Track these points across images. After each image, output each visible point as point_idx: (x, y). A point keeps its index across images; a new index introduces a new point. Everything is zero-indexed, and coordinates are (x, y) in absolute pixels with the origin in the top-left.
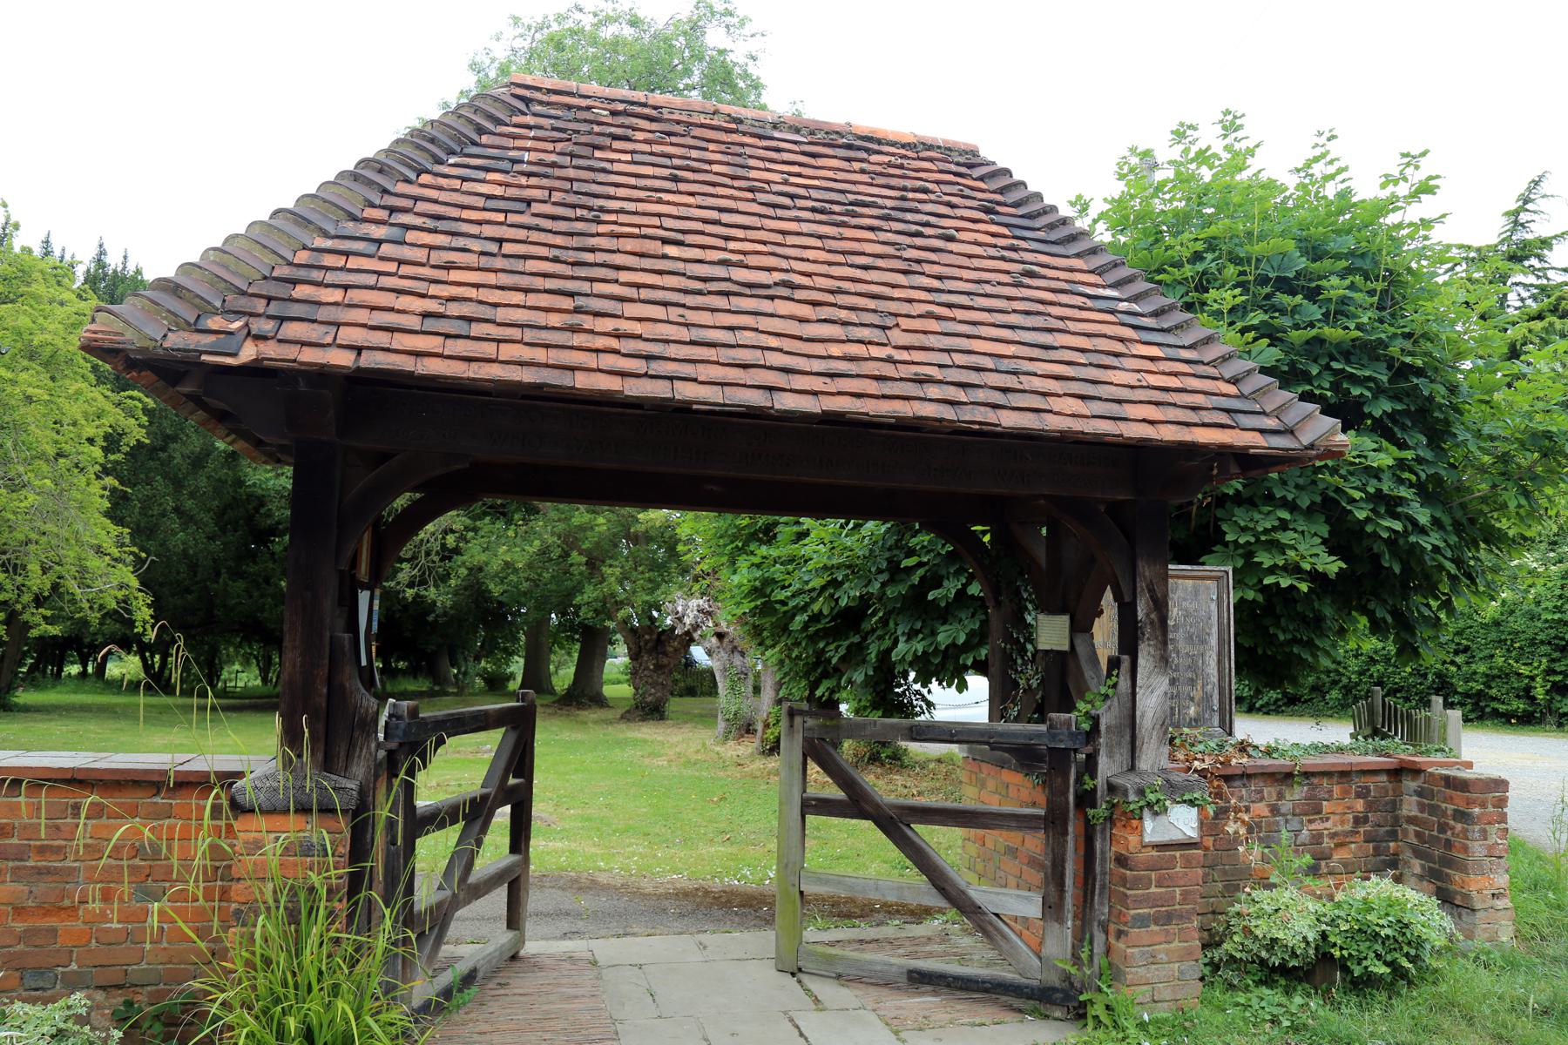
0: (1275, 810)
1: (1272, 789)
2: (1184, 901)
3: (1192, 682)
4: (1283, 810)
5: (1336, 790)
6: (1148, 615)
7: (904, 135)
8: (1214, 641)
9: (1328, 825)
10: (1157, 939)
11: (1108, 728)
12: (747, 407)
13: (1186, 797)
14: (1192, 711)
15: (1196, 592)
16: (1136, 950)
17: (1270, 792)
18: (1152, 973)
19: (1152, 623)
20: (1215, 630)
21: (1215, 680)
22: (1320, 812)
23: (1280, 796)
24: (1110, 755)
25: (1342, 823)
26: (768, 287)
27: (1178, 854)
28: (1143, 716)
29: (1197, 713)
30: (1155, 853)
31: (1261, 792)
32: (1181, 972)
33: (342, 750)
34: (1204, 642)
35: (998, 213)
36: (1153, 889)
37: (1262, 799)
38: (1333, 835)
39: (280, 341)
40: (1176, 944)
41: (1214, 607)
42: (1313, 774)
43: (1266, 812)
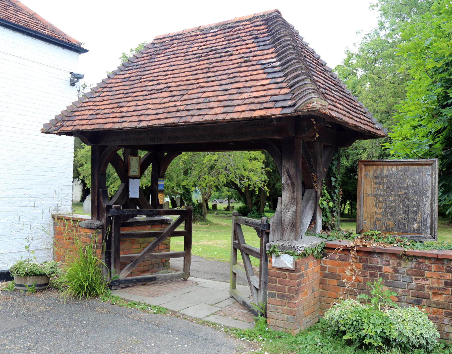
0: (396, 271)
1: (395, 261)
2: (289, 292)
3: (416, 213)
4: (400, 271)
5: (433, 267)
6: (286, 182)
7: (244, 17)
8: (429, 194)
9: (427, 282)
10: (278, 303)
11: (272, 225)
12: (164, 124)
13: (287, 252)
14: (415, 226)
15: (419, 171)
16: (270, 305)
17: (393, 262)
18: (276, 315)
19: (288, 184)
20: (429, 189)
21: (429, 212)
22: (423, 276)
23: (399, 265)
24: (274, 233)
25: (438, 283)
26: (162, 89)
27: (287, 273)
28: (284, 220)
29: (418, 227)
30: (278, 271)
31: (388, 261)
32: (287, 319)
33: (101, 216)
34: (423, 194)
35: (259, 38)
36: (277, 285)
37: (389, 265)
38: (430, 288)
39: (275, 108)
40: (286, 307)
41: (429, 178)
42: (418, 257)
43: (391, 271)
